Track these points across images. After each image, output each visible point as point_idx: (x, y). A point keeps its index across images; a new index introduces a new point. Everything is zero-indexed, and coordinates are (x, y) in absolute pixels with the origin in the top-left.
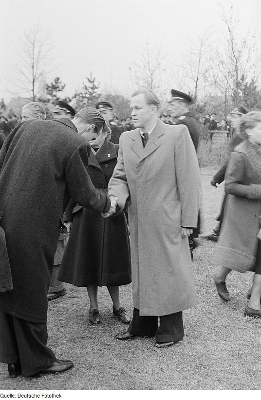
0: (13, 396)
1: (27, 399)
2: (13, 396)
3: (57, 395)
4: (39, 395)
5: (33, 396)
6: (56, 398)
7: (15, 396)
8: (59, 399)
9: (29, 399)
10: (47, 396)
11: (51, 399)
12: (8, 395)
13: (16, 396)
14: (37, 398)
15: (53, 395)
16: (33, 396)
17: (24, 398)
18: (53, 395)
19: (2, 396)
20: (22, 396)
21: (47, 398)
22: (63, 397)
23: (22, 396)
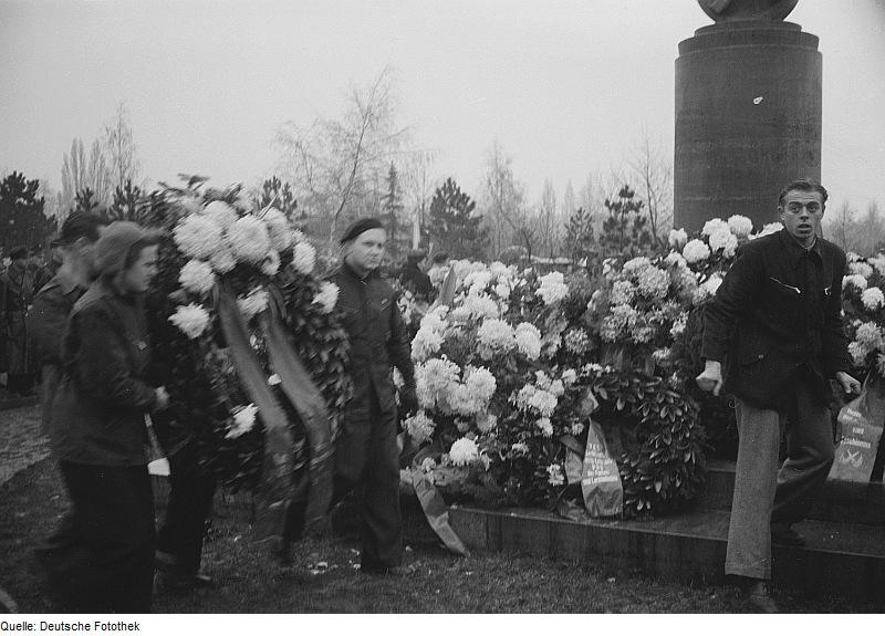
1: (61, 633)
2: (29, 627)
3: (131, 625)
5: (75, 627)
6: (128, 633)
8: (134, 632)
9: (66, 633)
11: (117, 633)
12: (19, 625)
13: (37, 627)
14: (85, 633)
16: (75, 627)
18: (121, 626)
19: (4, 626)
21: (107, 633)
22: (143, 630)
23: (51, 627)
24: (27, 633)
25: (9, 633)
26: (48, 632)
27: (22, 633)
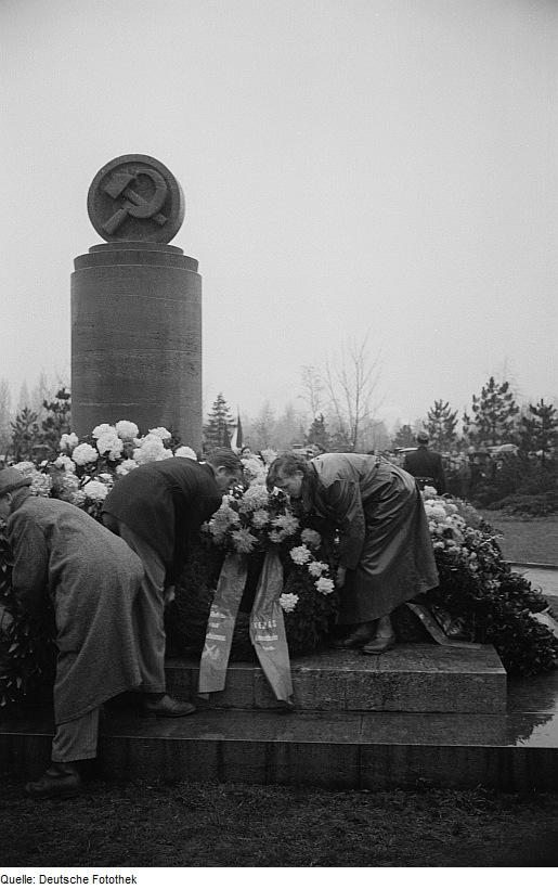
0: (28, 880)
1: (59, 886)
2: (28, 880)
3: (128, 879)
4: (86, 879)
5: (73, 880)
7: (34, 880)
9: (64, 886)
10: (106, 880)
12: (19, 879)
13: (37, 880)
14: (83, 886)
15: (118, 879)
16: (73, 880)
17: (53, 886)
18: (118, 879)
19: (4, 879)
20: (49, 880)
23: (49, 880)
24: (27, 886)
25: (9, 886)
26: (47, 885)
27: (22, 886)
